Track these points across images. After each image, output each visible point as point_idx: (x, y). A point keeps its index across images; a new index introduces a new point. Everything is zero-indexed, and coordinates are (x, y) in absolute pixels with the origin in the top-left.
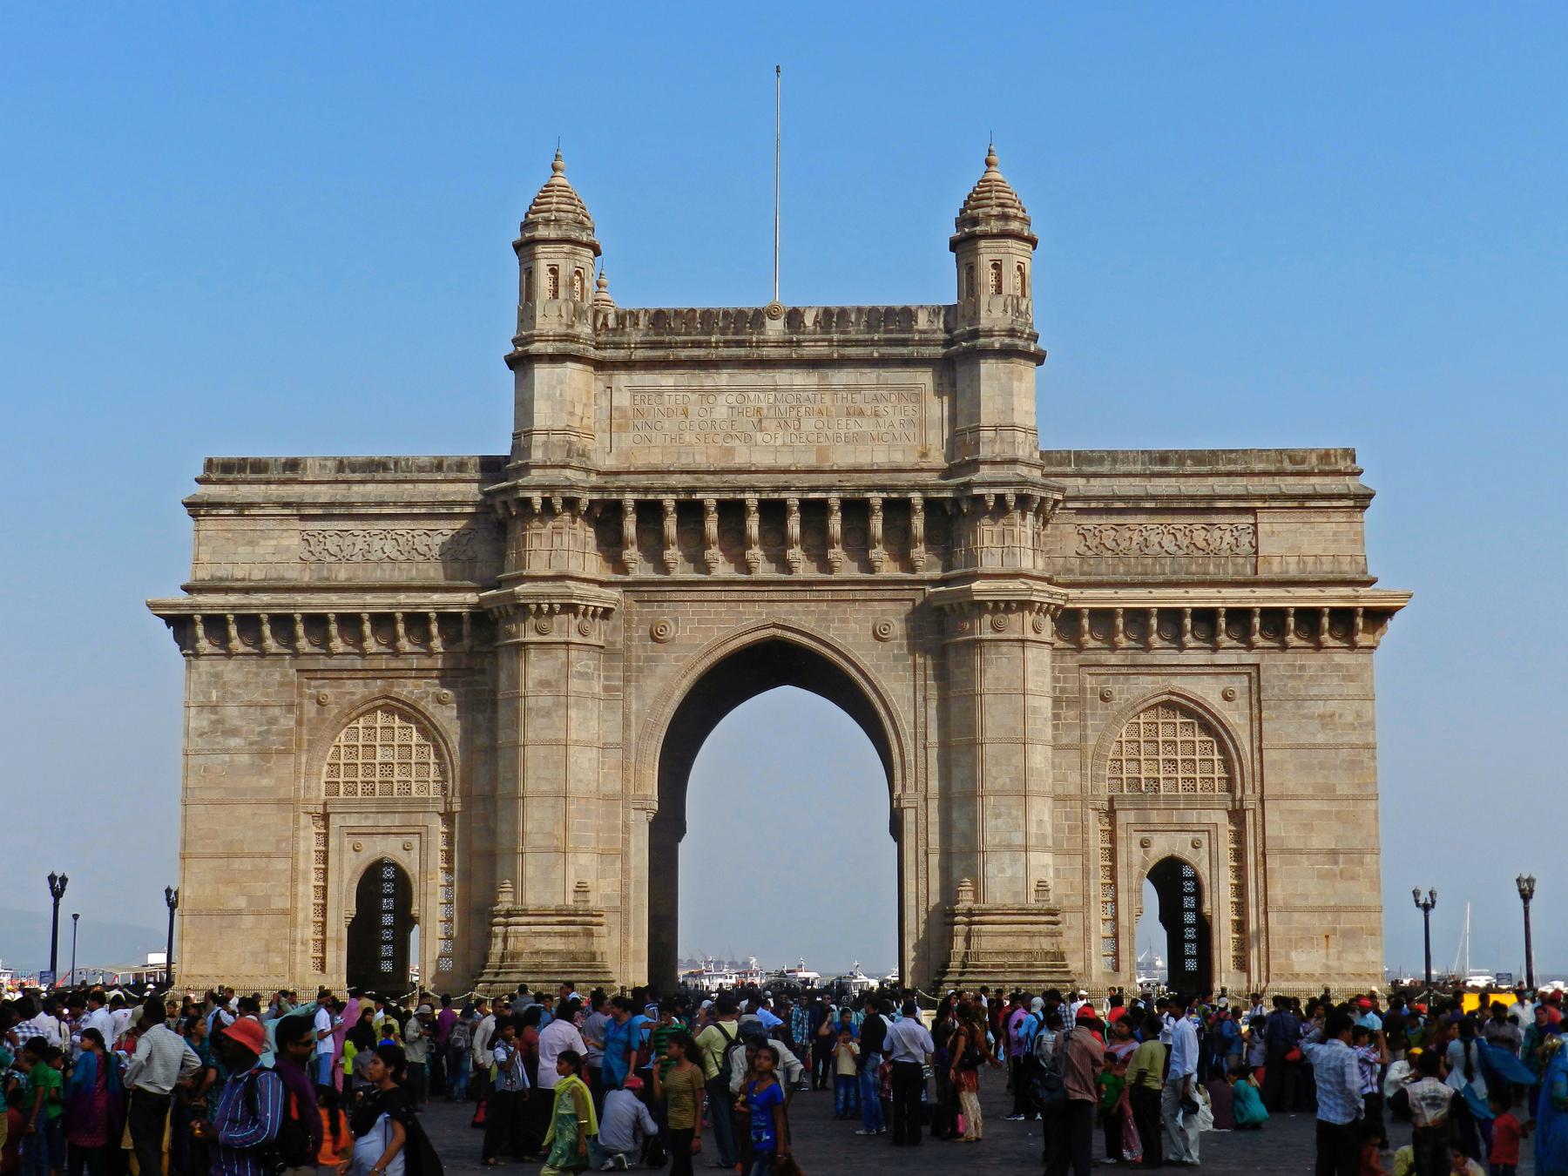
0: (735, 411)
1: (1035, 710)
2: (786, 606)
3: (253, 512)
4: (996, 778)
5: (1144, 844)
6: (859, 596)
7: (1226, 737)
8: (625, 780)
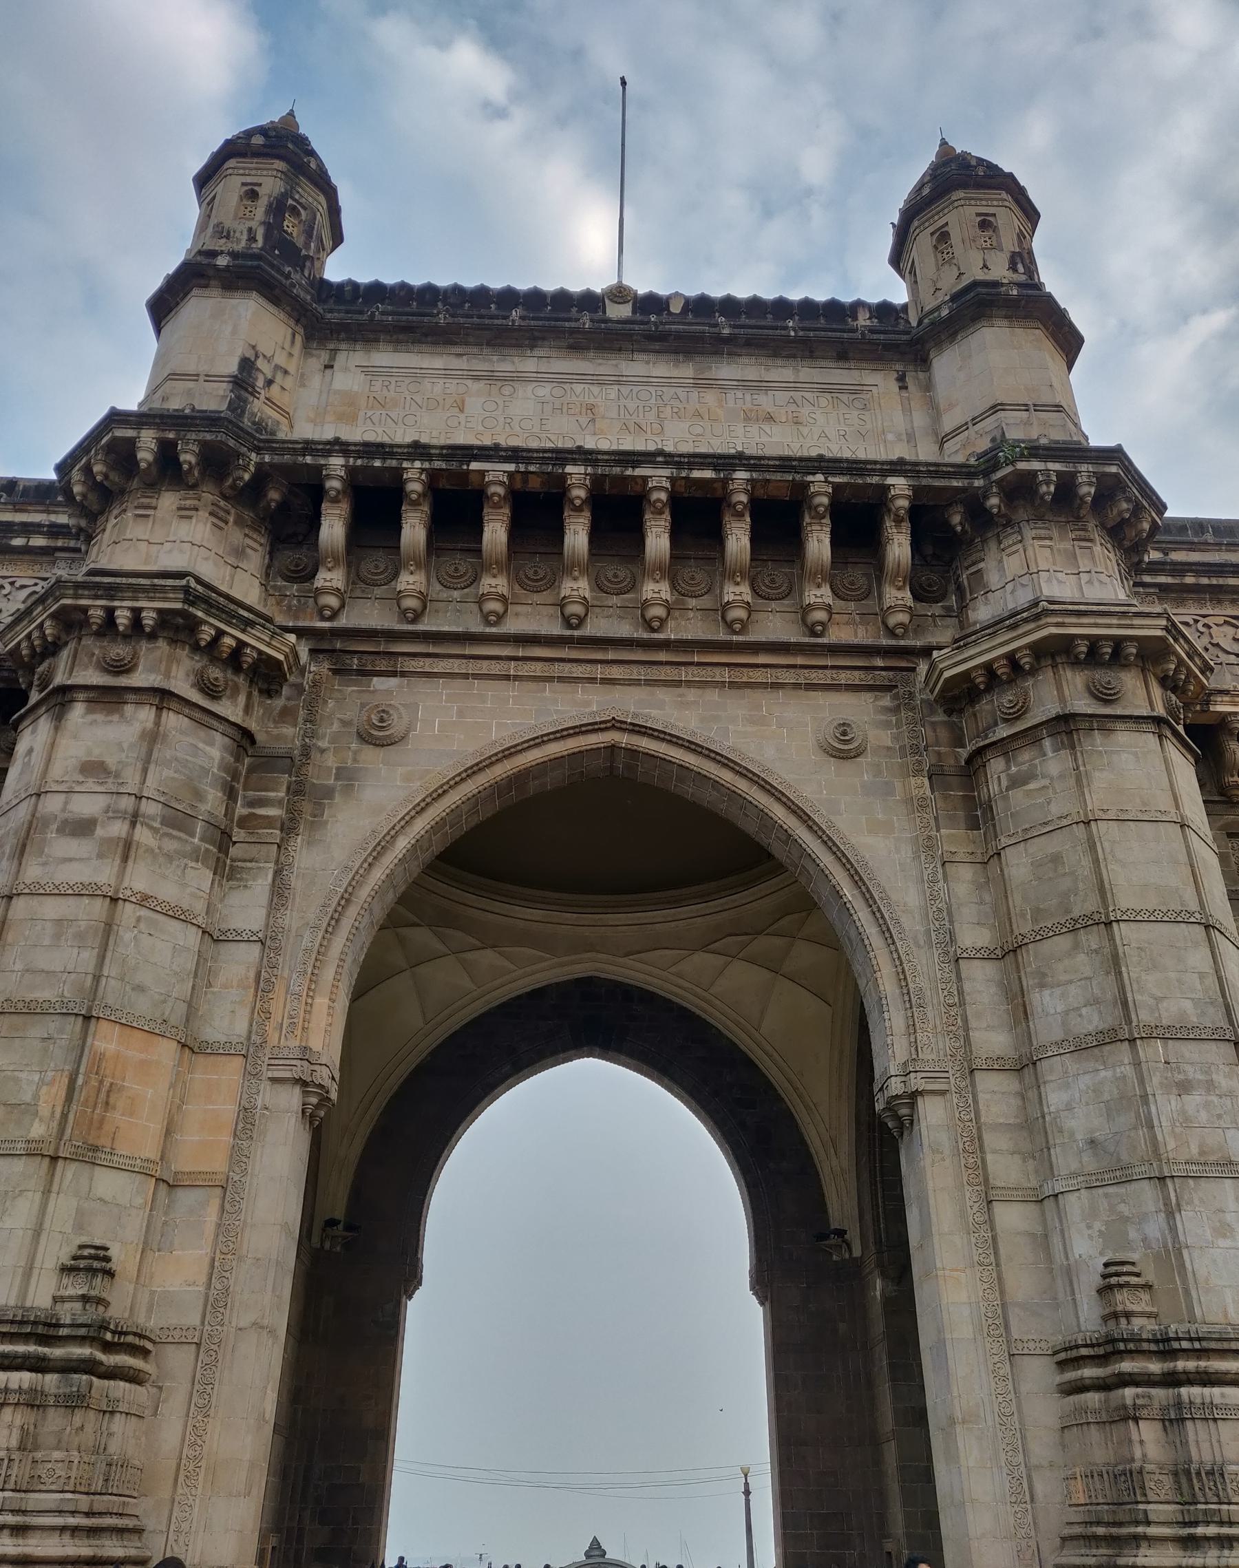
4: (1158, 1000)
6: (788, 677)
8: (260, 1013)
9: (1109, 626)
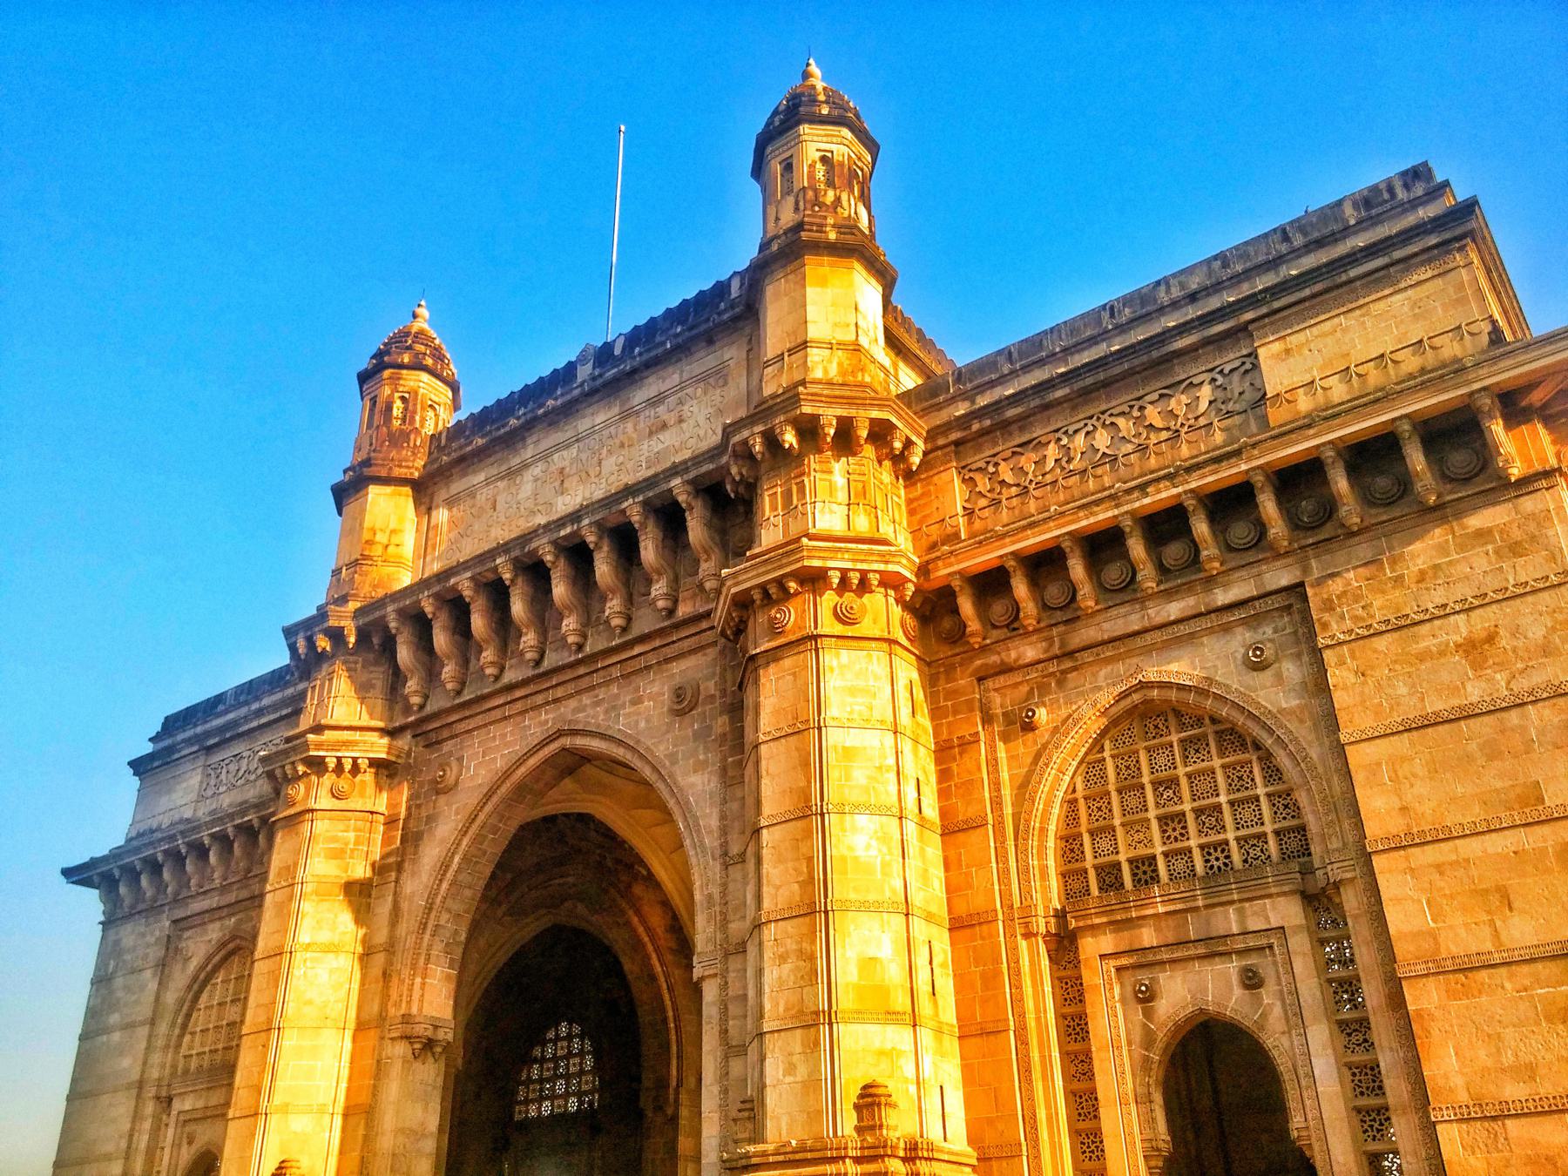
0: (539, 483)
1: (848, 753)
2: (573, 703)
3: (177, 756)
5: (1146, 998)
6: (652, 659)
7: (1268, 742)
9: (768, 572)
